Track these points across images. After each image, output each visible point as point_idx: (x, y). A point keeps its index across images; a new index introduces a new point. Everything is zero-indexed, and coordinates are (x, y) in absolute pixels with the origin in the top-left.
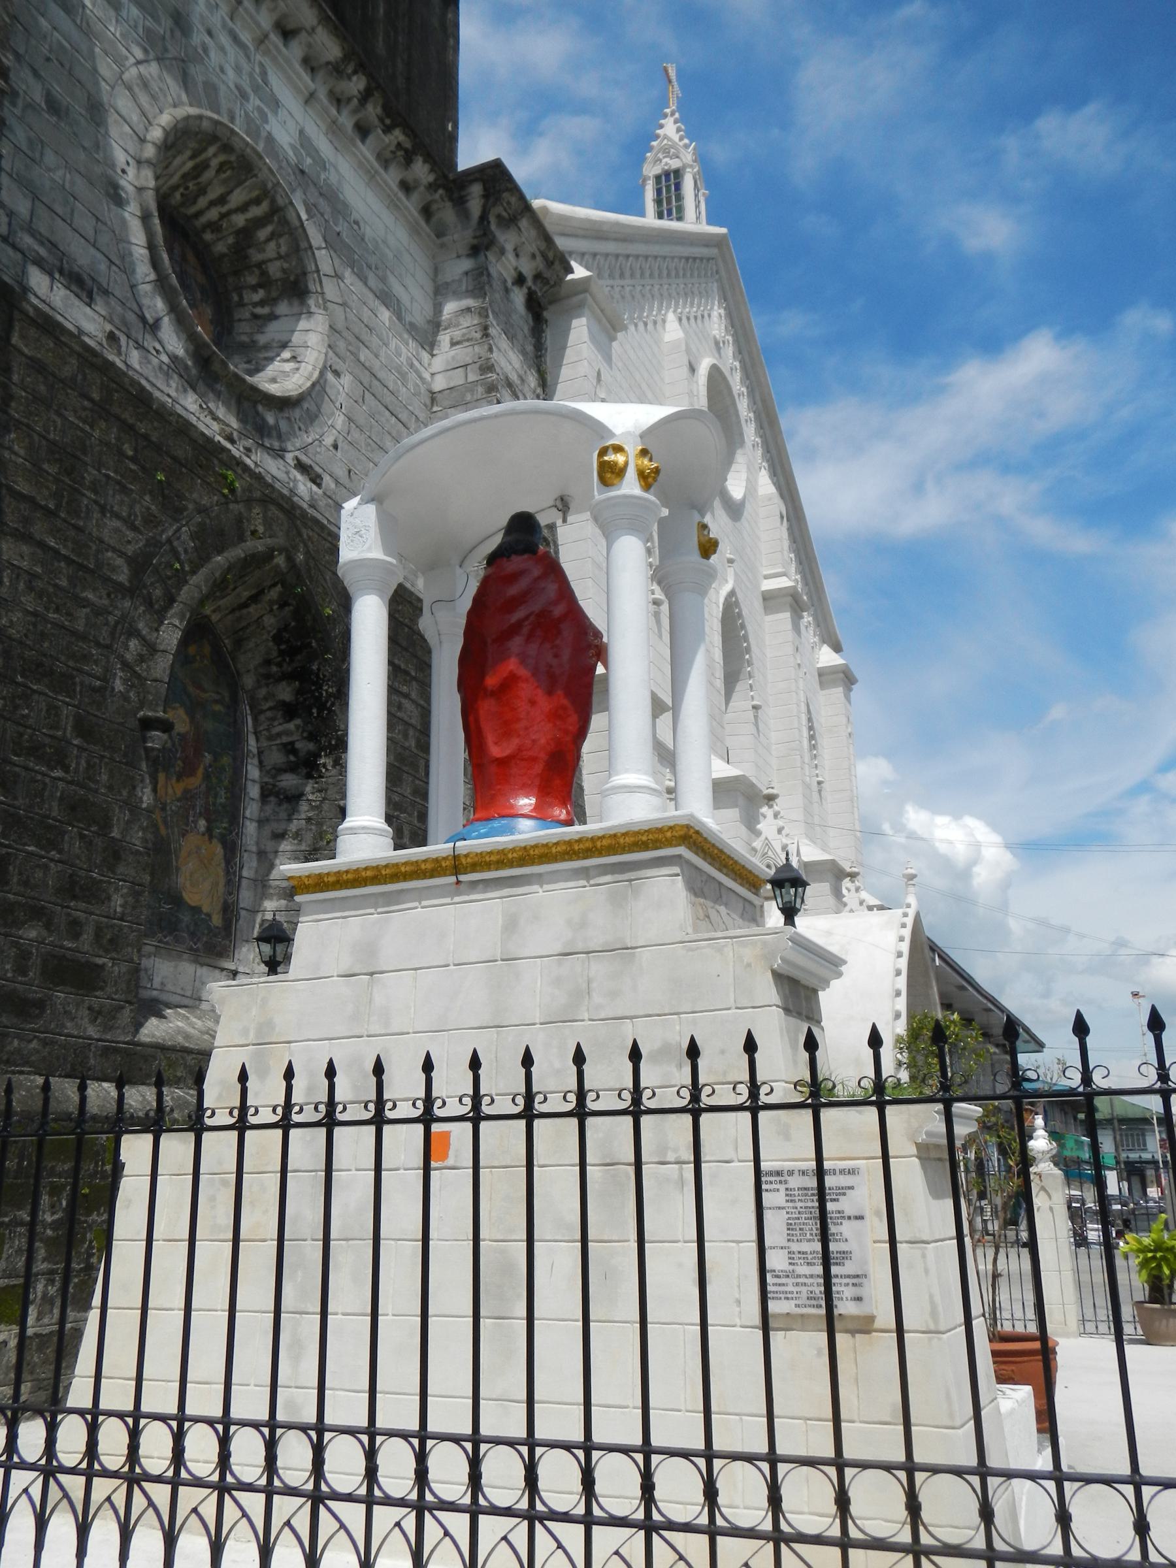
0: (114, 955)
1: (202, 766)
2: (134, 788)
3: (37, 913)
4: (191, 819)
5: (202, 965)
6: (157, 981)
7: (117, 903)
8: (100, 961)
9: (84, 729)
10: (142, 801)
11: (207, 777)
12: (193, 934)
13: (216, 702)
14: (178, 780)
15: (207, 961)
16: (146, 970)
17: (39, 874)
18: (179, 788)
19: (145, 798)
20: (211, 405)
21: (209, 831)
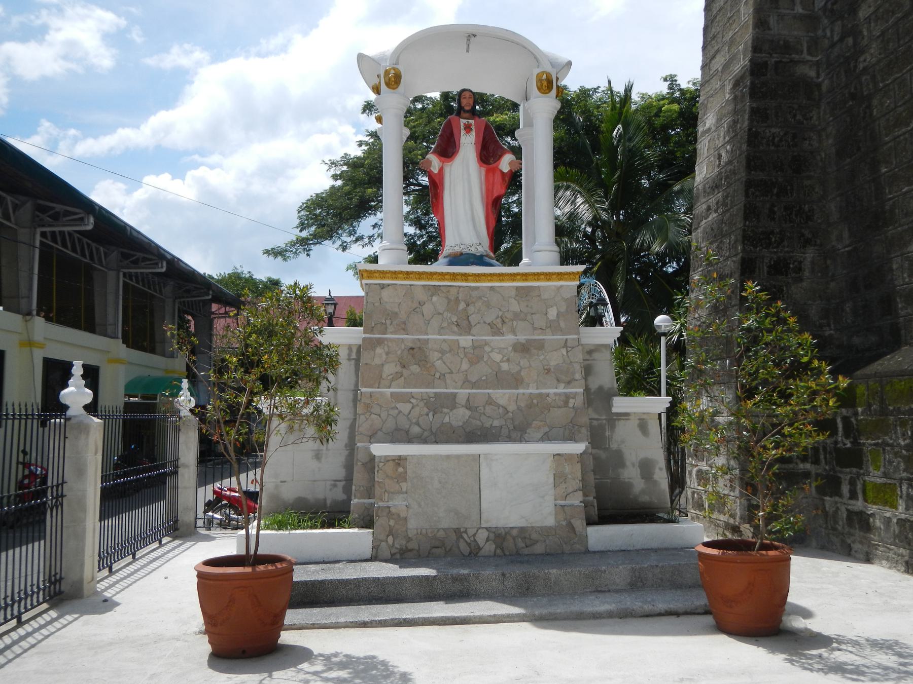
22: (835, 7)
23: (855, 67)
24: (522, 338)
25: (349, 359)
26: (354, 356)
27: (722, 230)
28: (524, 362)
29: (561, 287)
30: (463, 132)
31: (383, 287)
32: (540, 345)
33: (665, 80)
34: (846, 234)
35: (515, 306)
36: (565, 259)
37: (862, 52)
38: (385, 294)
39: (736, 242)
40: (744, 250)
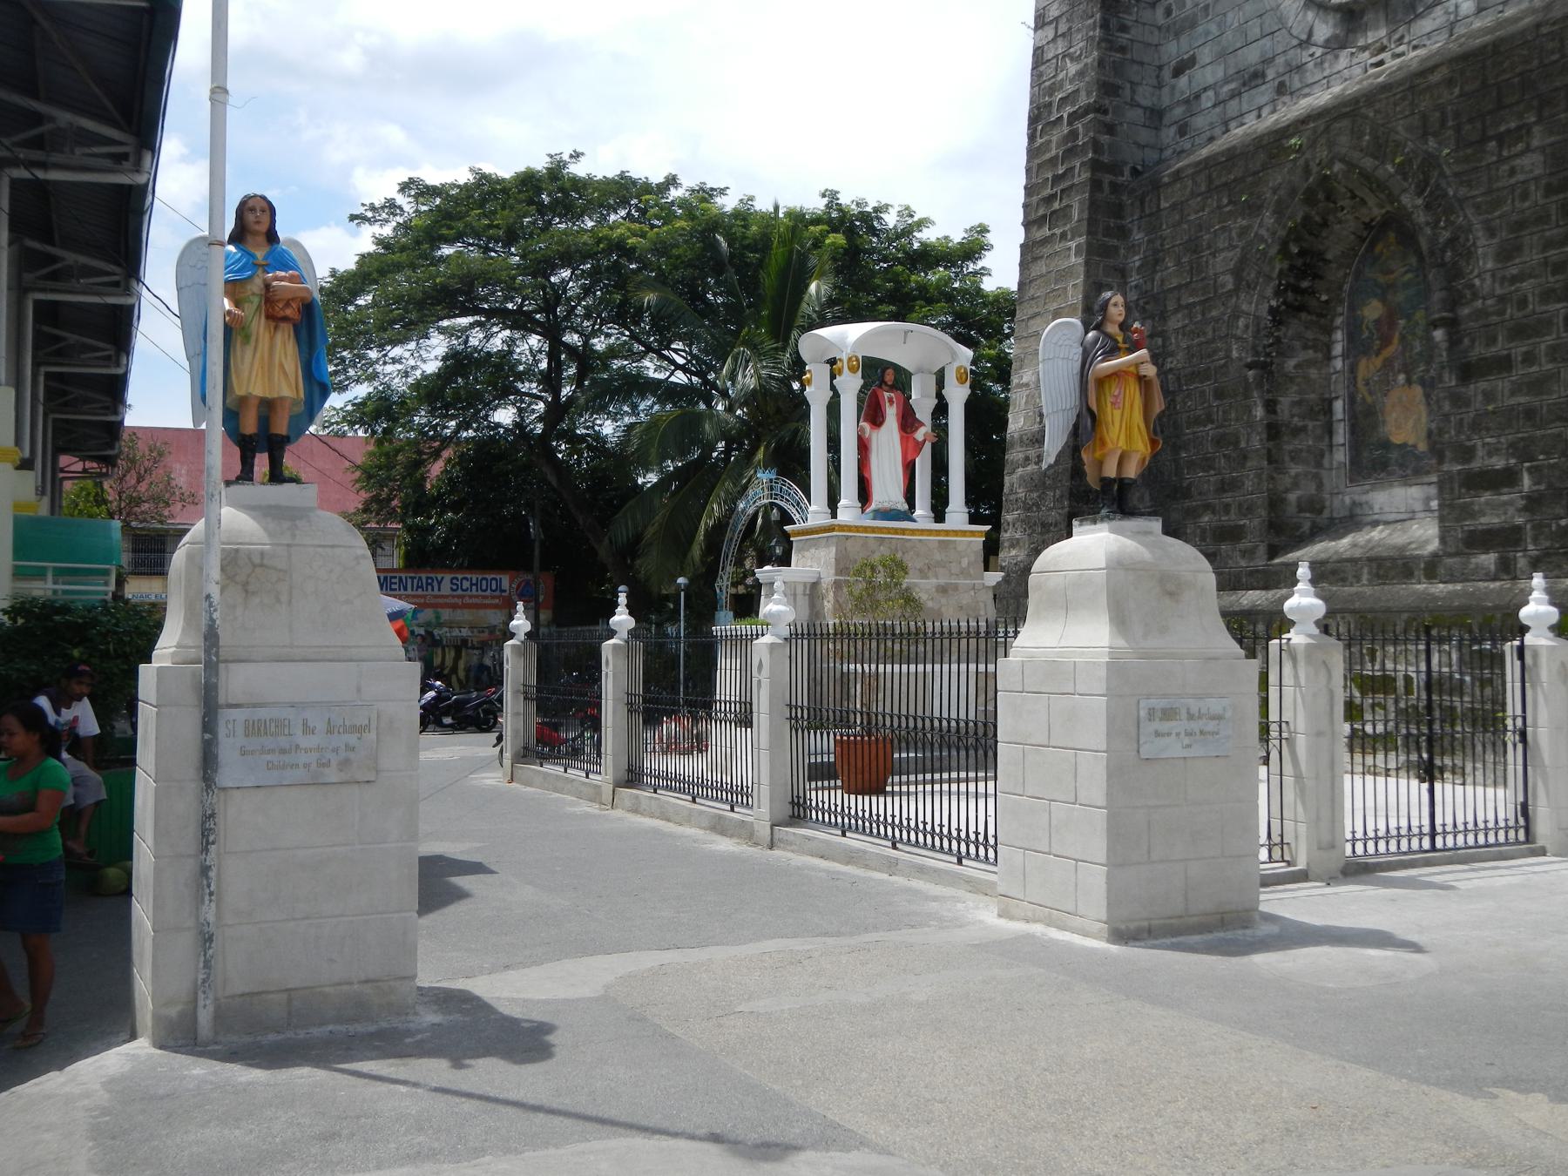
0: (1250, 516)
1: (1397, 335)
2: (1250, 411)
3: (1208, 507)
4: (1391, 378)
5: (1411, 486)
6: (1376, 510)
7: (1248, 485)
8: (1242, 523)
9: (1220, 394)
10: (1256, 416)
11: (1403, 338)
12: (1402, 466)
13: (1406, 272)
14: (1377, 355)
15: (1419, 481)
16: (1367, 503)
17: (1206, 486)
18: (1378, 362)
19: (1258, 414)
20: (1361, 43)
21: (1409, 382)
22: (1147, 307)
23: (1163, 364)
24: (942, 581)
25: (804, 595)
26: (808, 592)
27: (1044, 483)
28: (944, 601)
29: (971, 542)
30: (887, 404)
31: (847, 538)
32: (956, 588)
33: (824, 196)
34: (1147, 497)
35: (938, 557)
36: (973, 519)
37: (1172, 354)
38: (849, 543)
39: (1062, 496)
40: (1070, 506)
